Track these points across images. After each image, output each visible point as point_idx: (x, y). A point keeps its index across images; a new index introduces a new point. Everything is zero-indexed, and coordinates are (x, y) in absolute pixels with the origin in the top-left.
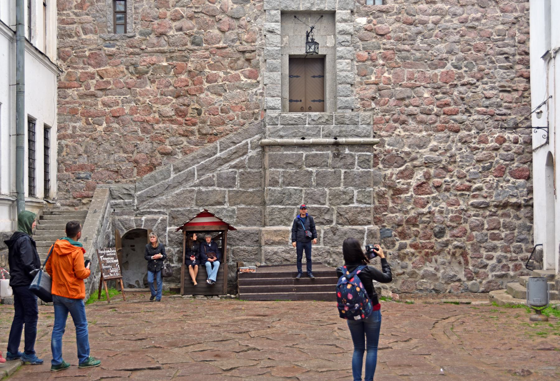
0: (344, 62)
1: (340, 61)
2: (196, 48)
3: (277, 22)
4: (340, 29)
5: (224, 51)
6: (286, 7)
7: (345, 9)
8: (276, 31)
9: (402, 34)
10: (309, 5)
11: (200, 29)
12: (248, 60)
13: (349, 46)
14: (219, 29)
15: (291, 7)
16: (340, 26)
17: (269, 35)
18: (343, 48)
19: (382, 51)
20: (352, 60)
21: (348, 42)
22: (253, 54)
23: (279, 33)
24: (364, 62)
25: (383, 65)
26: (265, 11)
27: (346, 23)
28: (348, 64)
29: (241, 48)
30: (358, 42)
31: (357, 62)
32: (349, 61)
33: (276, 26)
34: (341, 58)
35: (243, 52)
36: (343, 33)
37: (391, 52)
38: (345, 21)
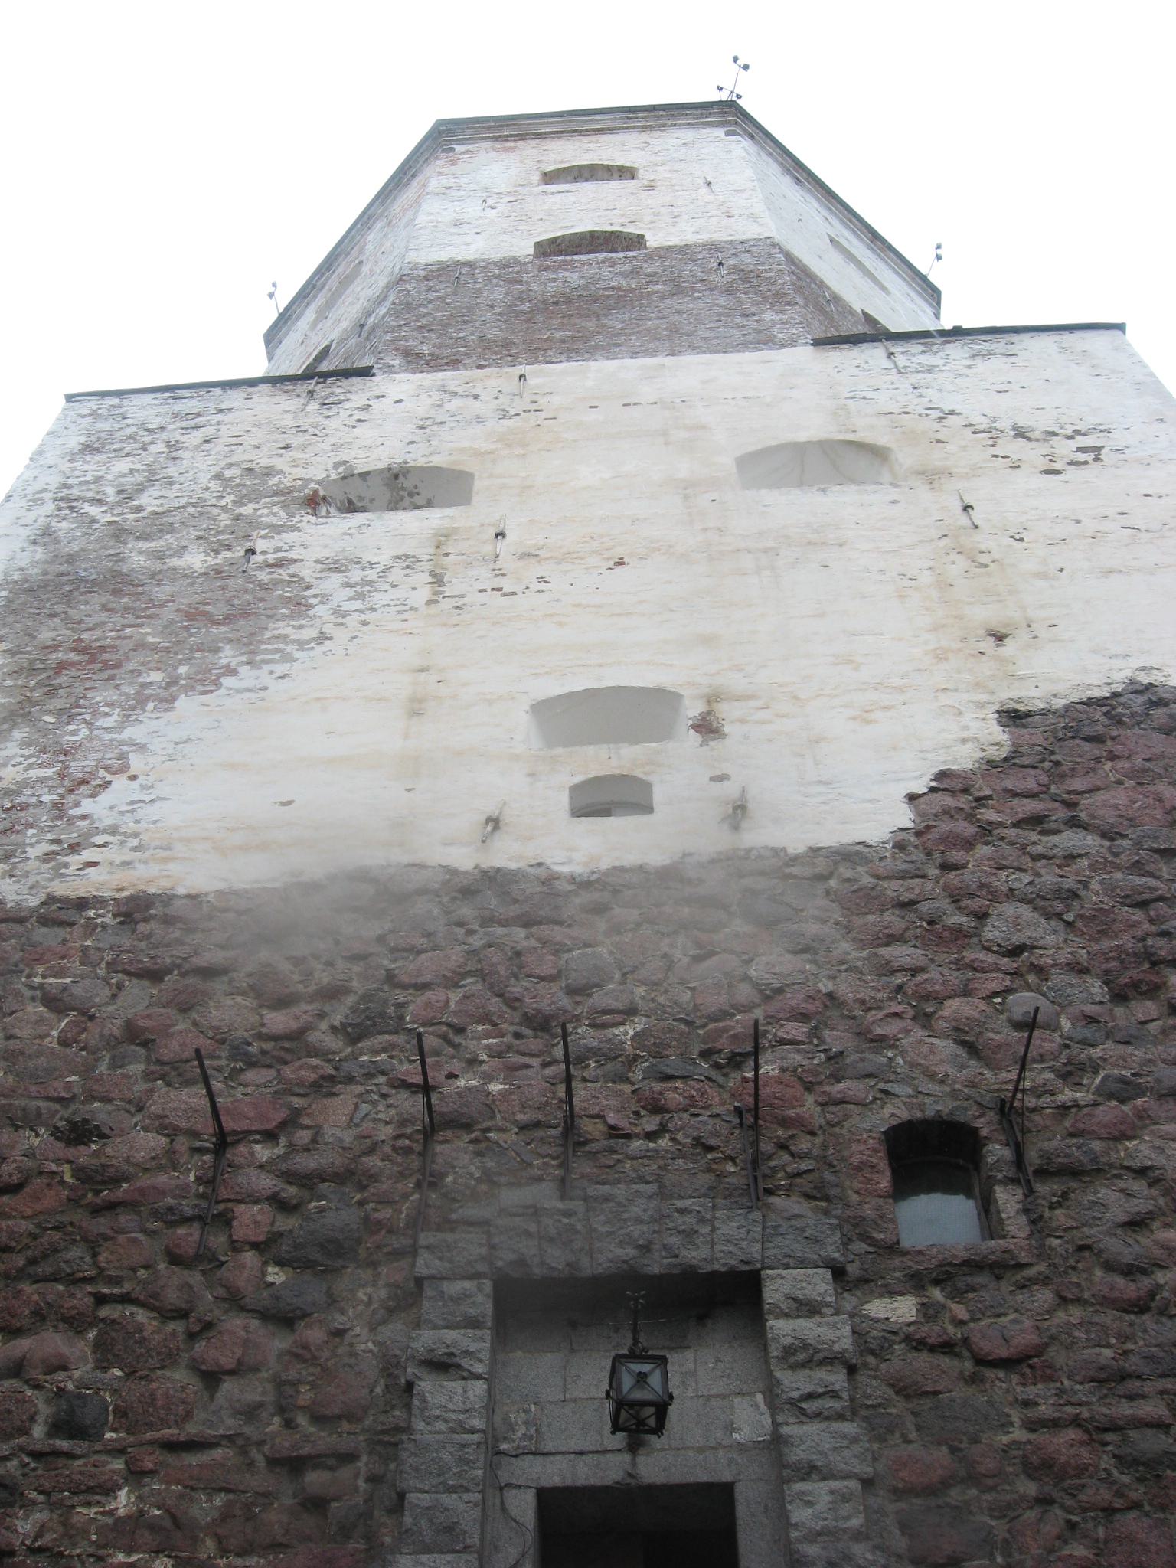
0: (821, 1491)
1: (799, 1486)
2: (63, 1444)
3: (473, 1323)
4: (788, 1341)
5: (193, 1459)
6: (521, 1262)
7: (803, 1263)
8: (464, 1363)
9: (1108, 1353)
10: (630, 1252)
11: (105, 1369)
12: (316, 1504)
13: (840, 1417)
14: (195, 1367)
15: (543, 1263)
16: (782, 1329)
17: (427, 1385)
18: (812, 1428)
19: (1019, 1434)
20: (867, 1483)
21: (834, 1395)
22: (345, 1473)
23: (479, 1368)
24: (930, 1490)
25: (1044, 1501)
26: (419, 1282)
27: (818, 1319)
28: (846, 1498)
29: (285, 1444)
30: (886, 1403)
31: (898, 1494)
32: (854, 1485)
33: (476, 1344)
34: (809, 1471)
35: (294, 1465)
36: (801, 1357)
37: (1072, 1434)
38: (808, 1308)
